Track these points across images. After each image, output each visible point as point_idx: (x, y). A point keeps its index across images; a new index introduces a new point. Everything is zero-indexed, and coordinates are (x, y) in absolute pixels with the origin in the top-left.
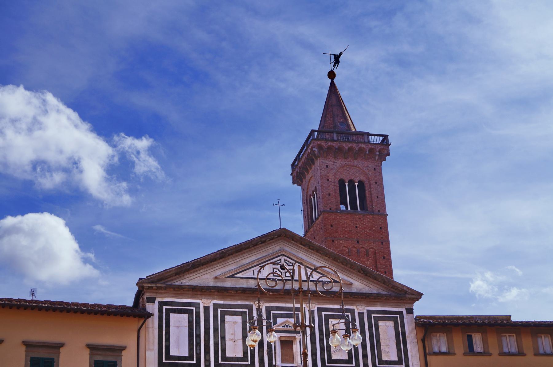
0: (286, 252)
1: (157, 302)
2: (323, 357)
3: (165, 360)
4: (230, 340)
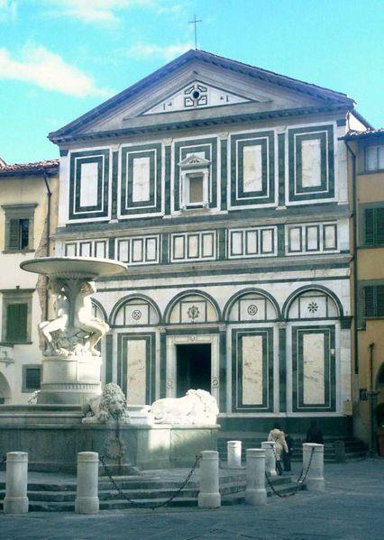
1: (69, 155)
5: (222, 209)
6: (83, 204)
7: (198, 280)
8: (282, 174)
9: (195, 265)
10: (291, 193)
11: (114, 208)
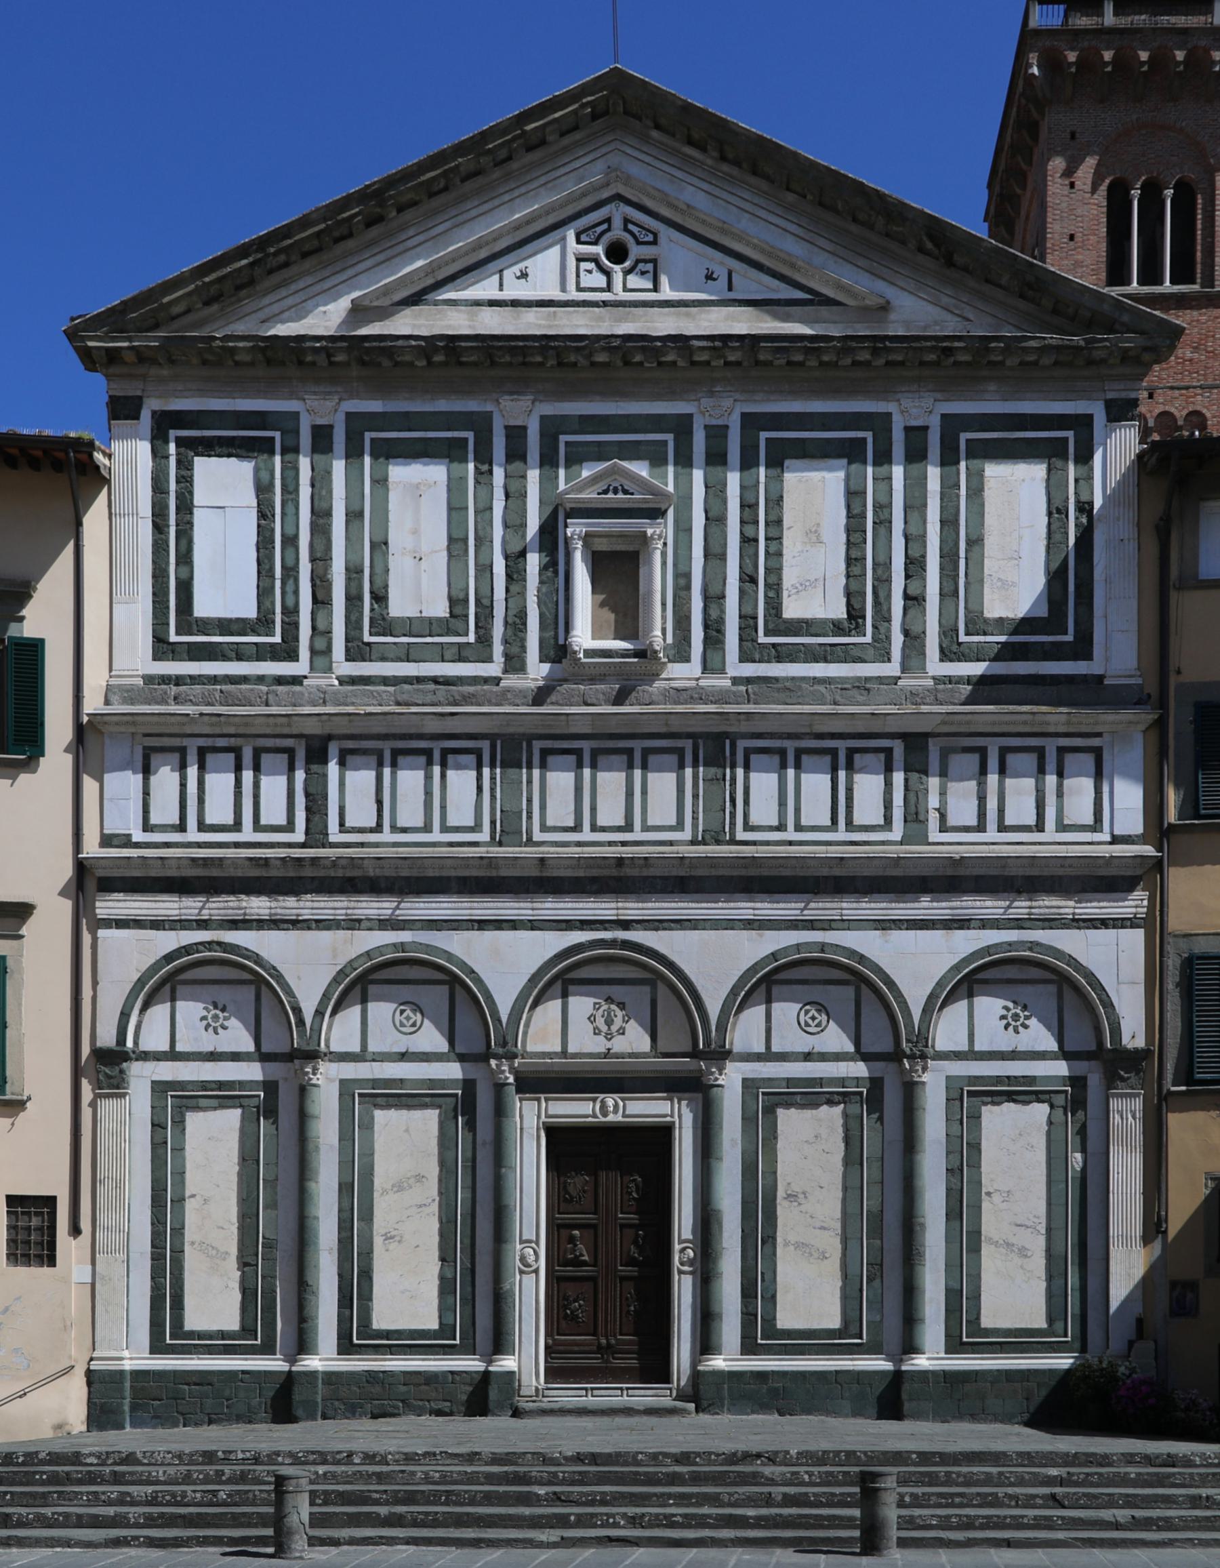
0: (627, 180)
2: (748, 610)
3: (178, 633)
5: (705, 668)
6: (204, 607)
7: (632, 909)
9: (627, 852)
10: (948, 631)
11: (321, 632)
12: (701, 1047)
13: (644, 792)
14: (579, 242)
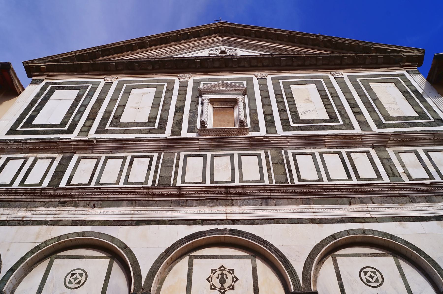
1: (43, 84)
4: (131, 108)
8: (353, 105)
12: (293, 291)
13: (240, 168)
14: (210, 51)
